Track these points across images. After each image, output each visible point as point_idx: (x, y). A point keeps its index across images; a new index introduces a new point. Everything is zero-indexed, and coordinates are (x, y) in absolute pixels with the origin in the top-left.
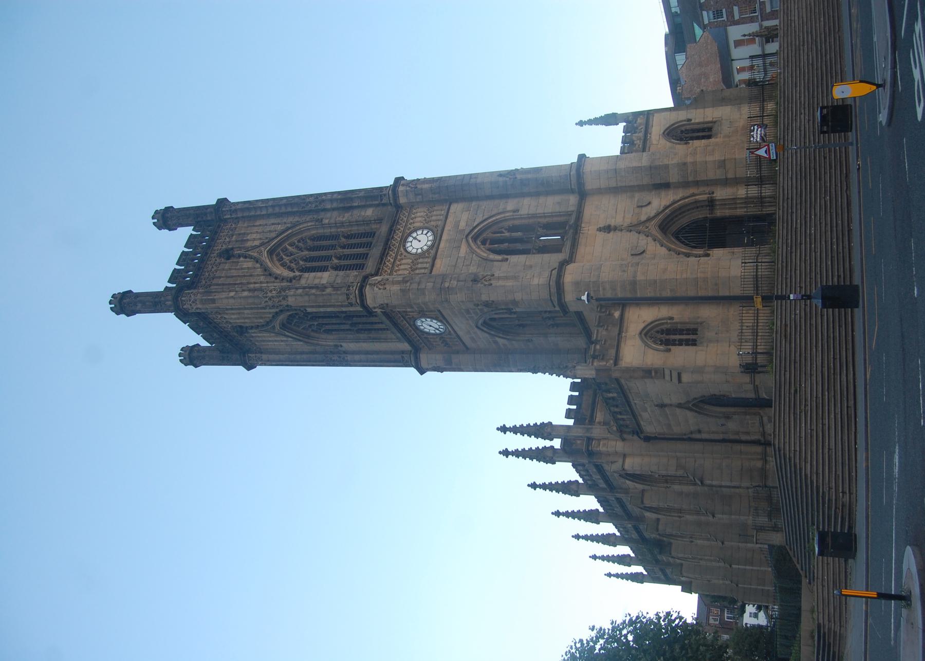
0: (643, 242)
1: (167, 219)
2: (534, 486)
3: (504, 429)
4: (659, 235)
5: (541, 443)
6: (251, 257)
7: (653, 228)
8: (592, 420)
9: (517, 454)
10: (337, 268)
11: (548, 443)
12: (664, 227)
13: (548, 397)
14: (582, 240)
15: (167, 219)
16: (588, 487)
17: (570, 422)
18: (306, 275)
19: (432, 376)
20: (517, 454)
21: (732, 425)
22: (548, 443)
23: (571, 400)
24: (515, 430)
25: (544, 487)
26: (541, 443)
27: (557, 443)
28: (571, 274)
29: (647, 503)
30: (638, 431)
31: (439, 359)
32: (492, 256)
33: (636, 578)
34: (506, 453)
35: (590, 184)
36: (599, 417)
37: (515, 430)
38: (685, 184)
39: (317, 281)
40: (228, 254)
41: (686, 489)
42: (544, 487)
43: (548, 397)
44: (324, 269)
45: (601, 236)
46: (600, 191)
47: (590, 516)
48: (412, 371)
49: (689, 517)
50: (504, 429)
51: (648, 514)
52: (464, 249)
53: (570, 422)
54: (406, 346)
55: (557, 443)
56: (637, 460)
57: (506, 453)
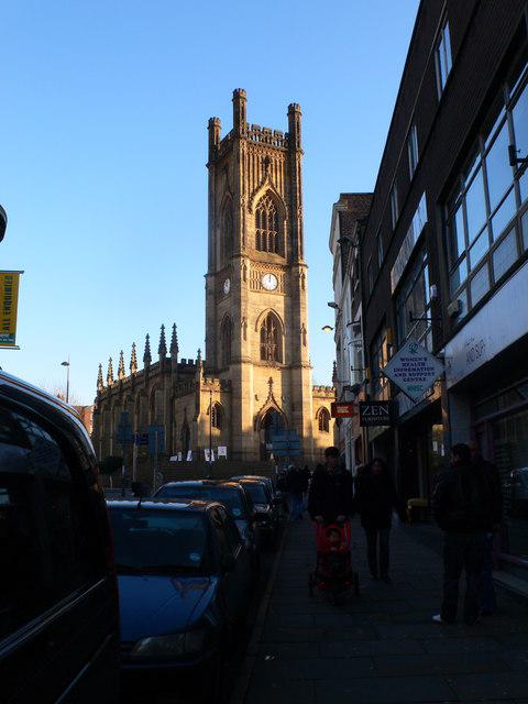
0: (263, 400)
1: (293, 112)
2: (148, 337)
3: (175, 327)
4: (267, 407)
5: (168, 347)
6: (264, 179)
7: (271, 404)
8: (179, 372)
9: (163, 334)
10: (258, 233)
11: (168, 350)
12: (271, 409)
13: (192, 347)
14: (266, 369)
15: (293, 112)
16: (148, 368)
17: (179, 362)
18: (254, 217)
19: (203, 281)
20: (163, 334)
21: (178, 442)
22: (168, 350)
23: (191, 361)
24: (174, 333)
25: (147, 343)
26: (168, 347)
27: (168, 355)
28: (251, 367)
29: (141, 398)
30: (174, 397)
31: (212, 287)
32: (259, 324)
33: (100, 381)
34: (163, 328)
35: (294, 371)
36: (182, 376)
37: (174, 333)
38: (292, 420)
39: (248, 224)
40: (267, 161)
41: (150, 417)
42: (147, 343)
43: (192, 347)
44: (258, 226)
45: (268, 379)
46: (291, 378)
47: (133, 364)
48: (206, 271)
49: (136, 417)
50: (175, 327)
51: (136, 396)
52: (264, 308)
53: (179, 362)
54: (218, 269)
55: (168, 355)
56: (162, 397)
57: (163, 328)
